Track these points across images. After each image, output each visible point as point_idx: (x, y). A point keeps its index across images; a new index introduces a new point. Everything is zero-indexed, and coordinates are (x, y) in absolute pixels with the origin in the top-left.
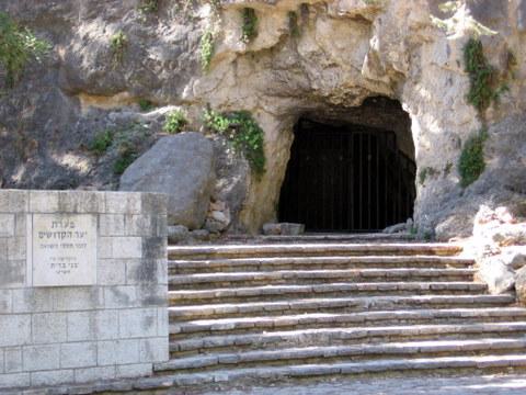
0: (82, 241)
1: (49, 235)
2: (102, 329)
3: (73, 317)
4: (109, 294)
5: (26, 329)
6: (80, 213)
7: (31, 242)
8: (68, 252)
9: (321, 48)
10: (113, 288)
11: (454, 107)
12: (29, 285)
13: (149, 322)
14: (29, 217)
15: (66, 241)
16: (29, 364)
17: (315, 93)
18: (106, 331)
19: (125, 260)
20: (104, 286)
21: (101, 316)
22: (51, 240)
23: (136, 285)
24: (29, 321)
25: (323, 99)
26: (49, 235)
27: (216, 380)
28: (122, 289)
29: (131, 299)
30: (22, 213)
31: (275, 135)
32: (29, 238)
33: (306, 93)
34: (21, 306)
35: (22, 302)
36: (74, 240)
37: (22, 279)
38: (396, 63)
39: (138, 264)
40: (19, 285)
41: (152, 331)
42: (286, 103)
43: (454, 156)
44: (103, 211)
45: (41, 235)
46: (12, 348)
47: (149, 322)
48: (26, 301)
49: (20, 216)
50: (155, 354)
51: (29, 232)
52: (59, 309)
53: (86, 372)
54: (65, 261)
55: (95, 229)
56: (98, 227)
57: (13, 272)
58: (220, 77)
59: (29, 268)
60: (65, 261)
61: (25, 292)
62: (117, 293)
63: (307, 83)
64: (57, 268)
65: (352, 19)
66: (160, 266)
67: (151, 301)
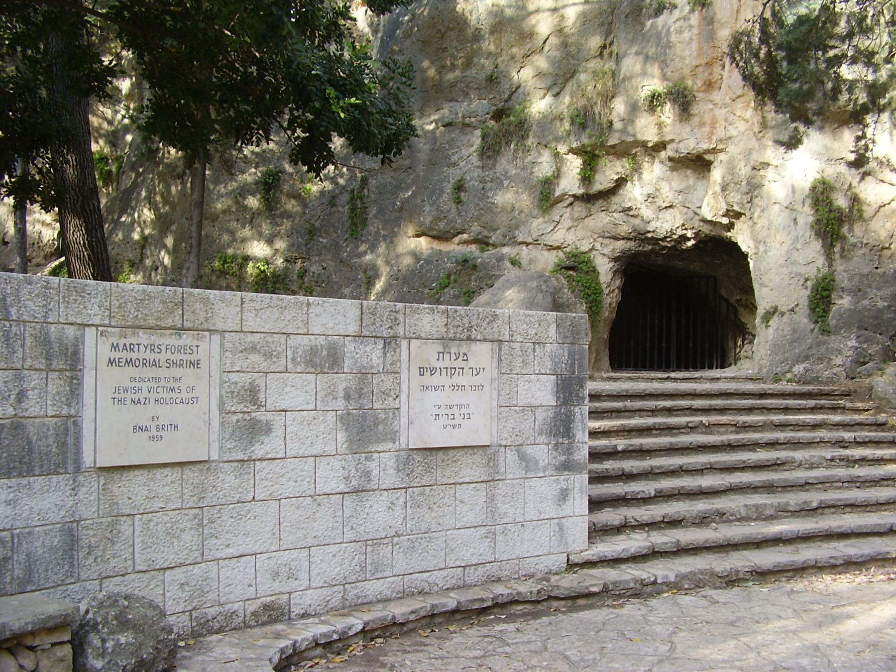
0: (477, 380)
1: (433, 371)
2: (503, 508)
3: (463, 492)
4: (511, 457)
5: (398, 511)
6: (475, 340)
7: (409, 379)
8: (458, 397)
9: (658, 190)
10: (519, 448)
11: (799, 246)
12: (403, 446)
13: (564, 495)
14: (404, 343)
15: (457, 380)
16: (401, 563)
17: (649, 235)
18: (508, 509)
19: (533, 408)
20: (505, 446)
21: (502, 488)
22: (436, 380)
23: (547, 444)
24: (401, 501)
25: (654, 240)
26: (433, 371)
27: (659, 581)
28: (529, 450)
29: (541, 464)
30: (395, 337)
31: (610, 276)
32: (404, 376)
33: (640, 236)
34: (390, 478)
35: (392, 472)
36: (465, 380)
37: (393, 437)
38: (738, 204)
39: (551, 414)
40: (390, 445)
41: (567, 509)
42: (620, 245)
43: (802, 296)
44: (507, 338)
45: (422, 371)
46: (377, 542)
47: (564, 495)
48: (398, 471)
49: (390, 342)
50: (570, 540)
51: (404, 366)
52: (445, 481)
53: (481, 570)
54: (455, 410)
55: (495, 364)
56: (500, 360)
57: (380, 427)
58: (557, 218)
59: (404, 420)
60: (455, 410)
61: (397, 457)
62: (523, 457)
63: (642, 226)
64: (443, 420)
65: (692, 160)
66: (578, 416)
67: (567, 467)
